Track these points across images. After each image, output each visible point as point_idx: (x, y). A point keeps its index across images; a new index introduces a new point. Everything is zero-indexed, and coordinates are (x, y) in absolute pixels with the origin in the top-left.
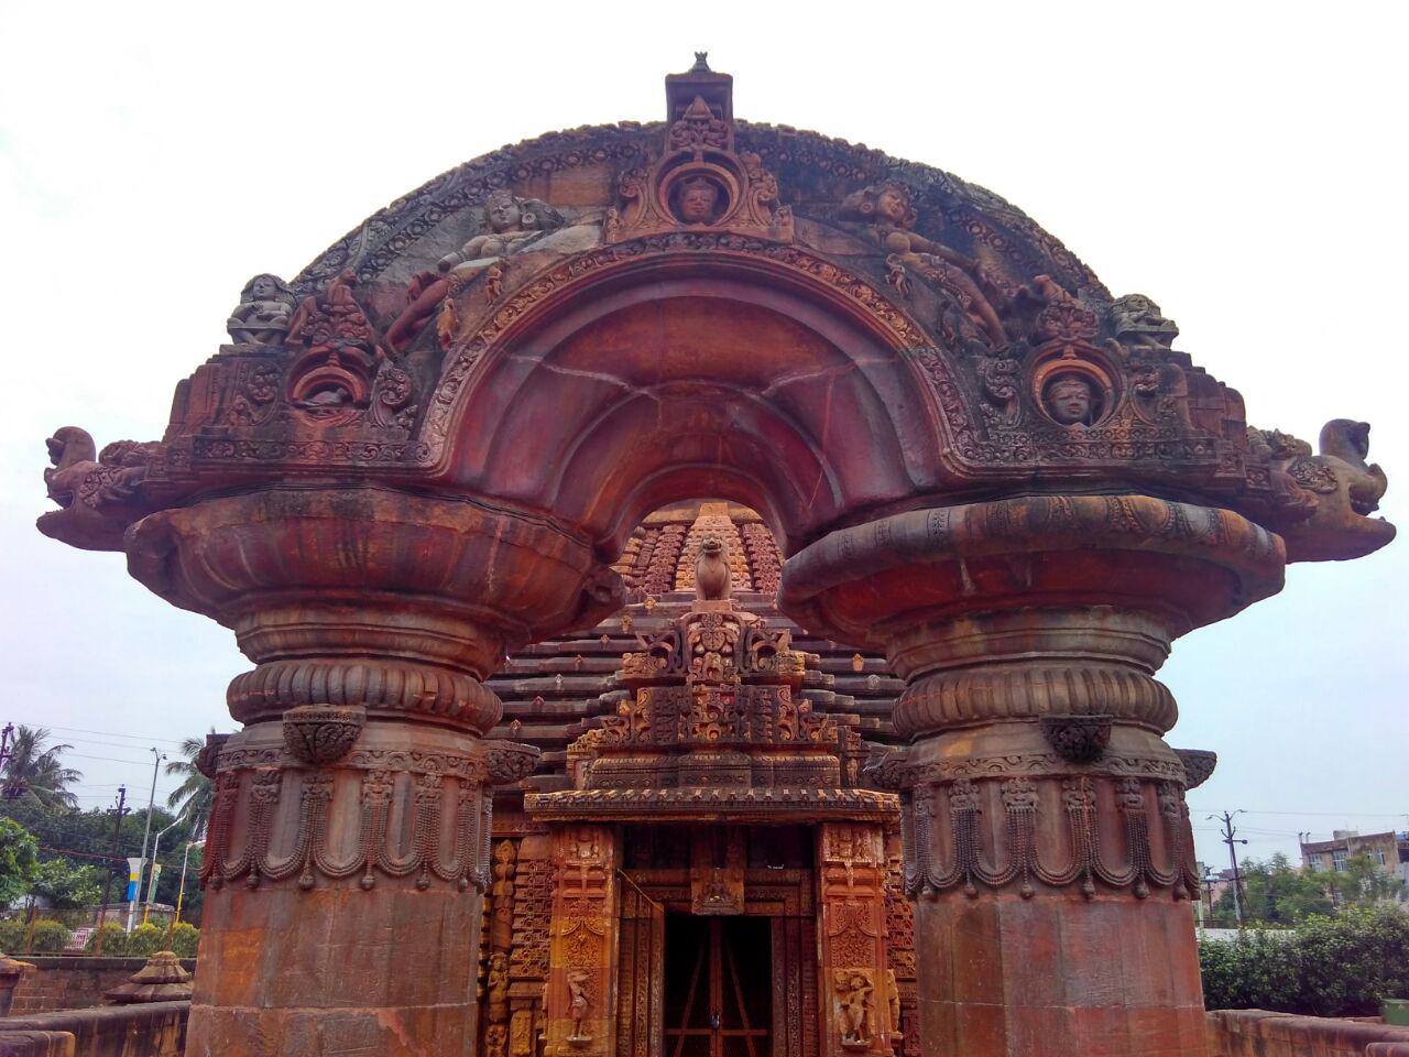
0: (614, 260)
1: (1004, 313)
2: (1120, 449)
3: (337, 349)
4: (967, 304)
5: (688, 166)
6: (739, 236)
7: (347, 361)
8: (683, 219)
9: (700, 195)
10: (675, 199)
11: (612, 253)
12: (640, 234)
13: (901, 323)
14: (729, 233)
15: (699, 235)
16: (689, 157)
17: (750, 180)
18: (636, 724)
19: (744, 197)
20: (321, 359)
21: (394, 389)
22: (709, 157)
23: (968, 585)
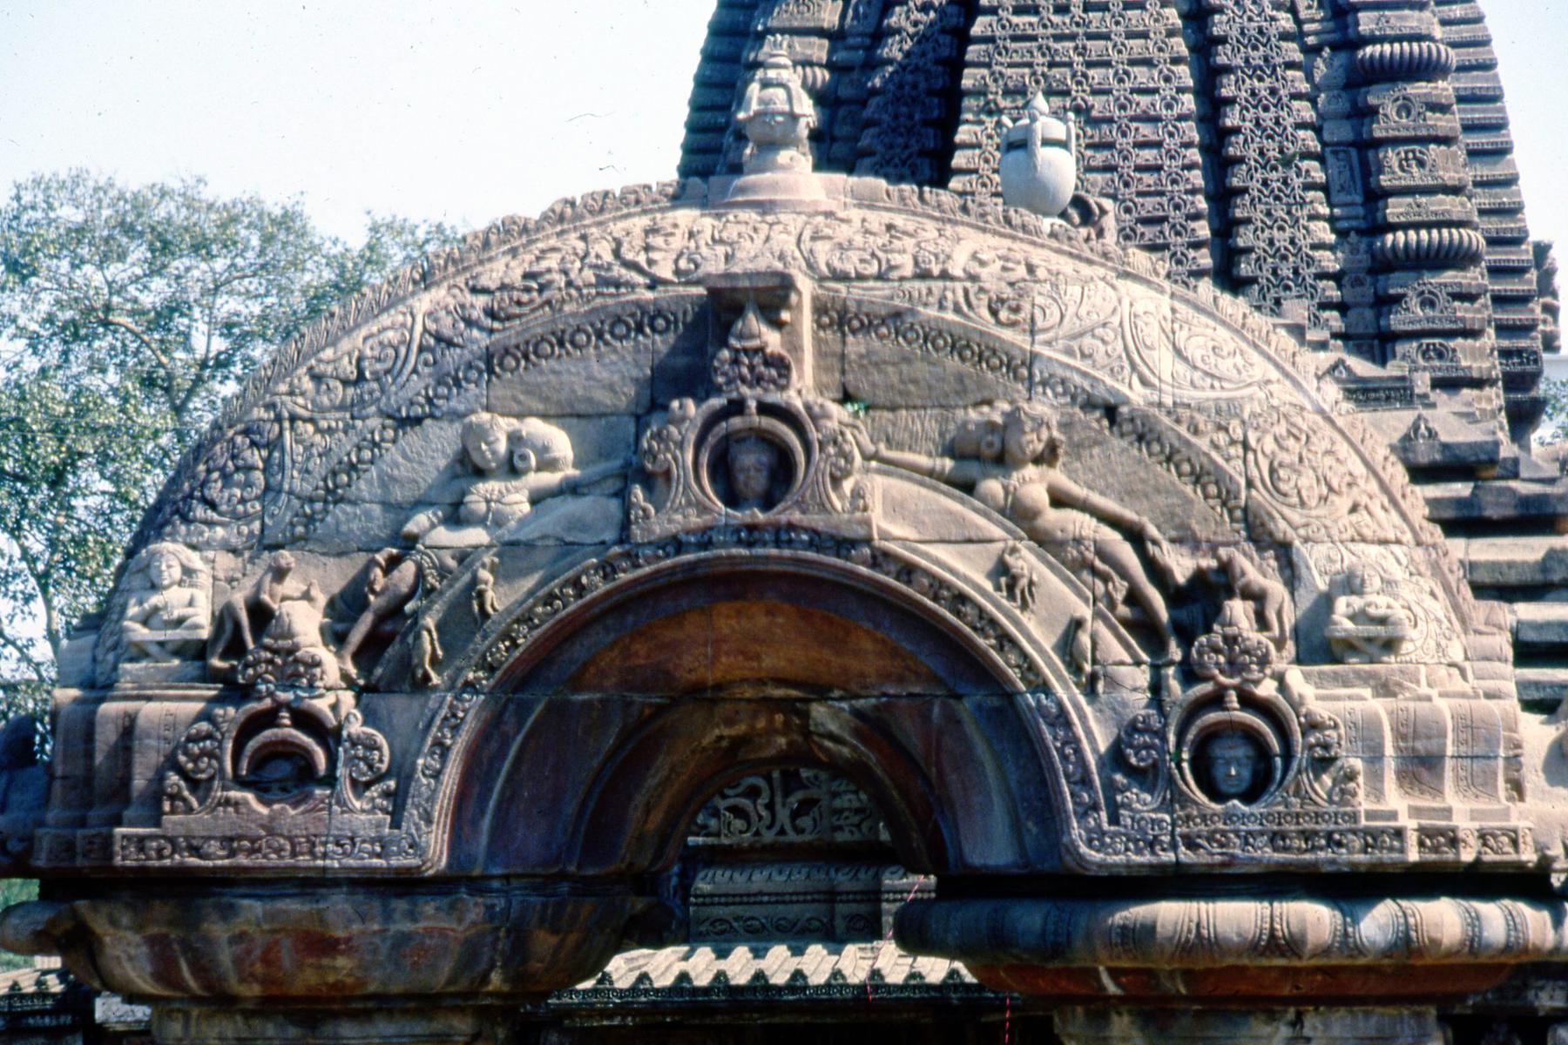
0: (638, 566)
1: (1175, 596)
2: (1283, 839)
3: (287, 706)
4: (1119, 597)
5: (736, 422)
6: (806, 530)
7: (307, 721)
8: (732, 498)
9: (751, 461)
10: (723, 471)
11: (637, 556)
12: (673, 528)
13: (1013, 658)
14: (791, 526)
15: (752, 528)
16: (737, 407)
17: (820, 443)
18: (786, 794)
19: (812, 470)
20: (268, 719)
21: (364, 759)
22: (765, 409)
23: (1112, 988)
